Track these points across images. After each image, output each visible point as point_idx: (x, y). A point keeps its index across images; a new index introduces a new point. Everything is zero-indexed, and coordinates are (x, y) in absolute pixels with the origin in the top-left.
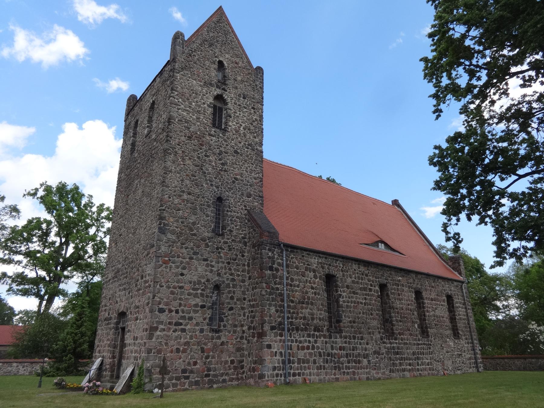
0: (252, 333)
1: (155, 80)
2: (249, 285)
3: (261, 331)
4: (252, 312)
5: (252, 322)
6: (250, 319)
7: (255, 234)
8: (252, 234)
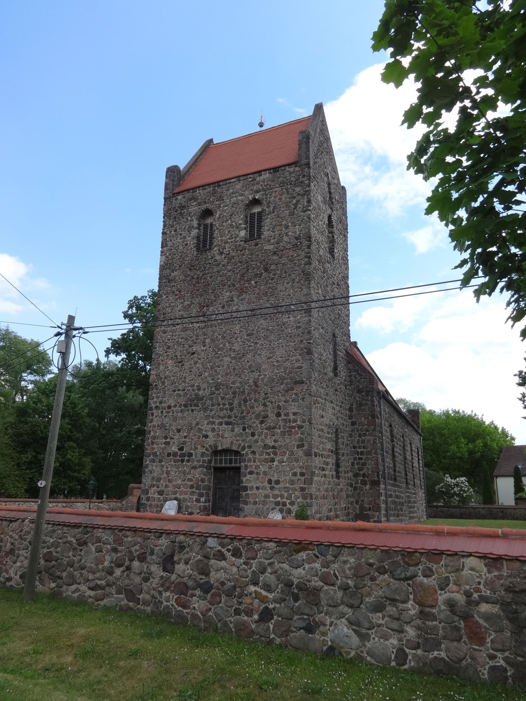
0: (361, 480)
1: (259, 172)
2: (353, 431)
3: (376, 479)
4: (360, 459)
5: (360, 469)
6: (356, 467)
7: (361, 378)
8: (356, 378)
